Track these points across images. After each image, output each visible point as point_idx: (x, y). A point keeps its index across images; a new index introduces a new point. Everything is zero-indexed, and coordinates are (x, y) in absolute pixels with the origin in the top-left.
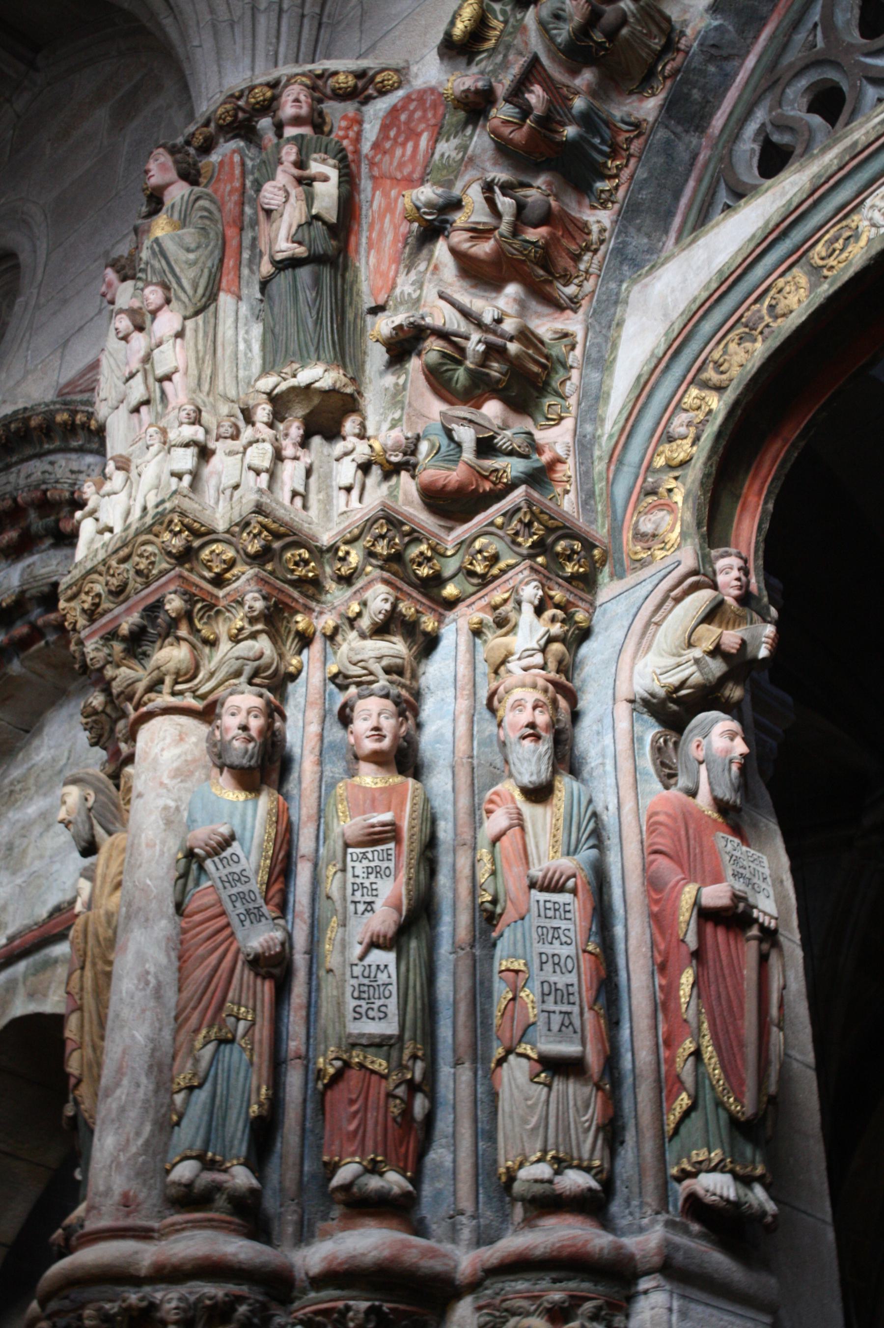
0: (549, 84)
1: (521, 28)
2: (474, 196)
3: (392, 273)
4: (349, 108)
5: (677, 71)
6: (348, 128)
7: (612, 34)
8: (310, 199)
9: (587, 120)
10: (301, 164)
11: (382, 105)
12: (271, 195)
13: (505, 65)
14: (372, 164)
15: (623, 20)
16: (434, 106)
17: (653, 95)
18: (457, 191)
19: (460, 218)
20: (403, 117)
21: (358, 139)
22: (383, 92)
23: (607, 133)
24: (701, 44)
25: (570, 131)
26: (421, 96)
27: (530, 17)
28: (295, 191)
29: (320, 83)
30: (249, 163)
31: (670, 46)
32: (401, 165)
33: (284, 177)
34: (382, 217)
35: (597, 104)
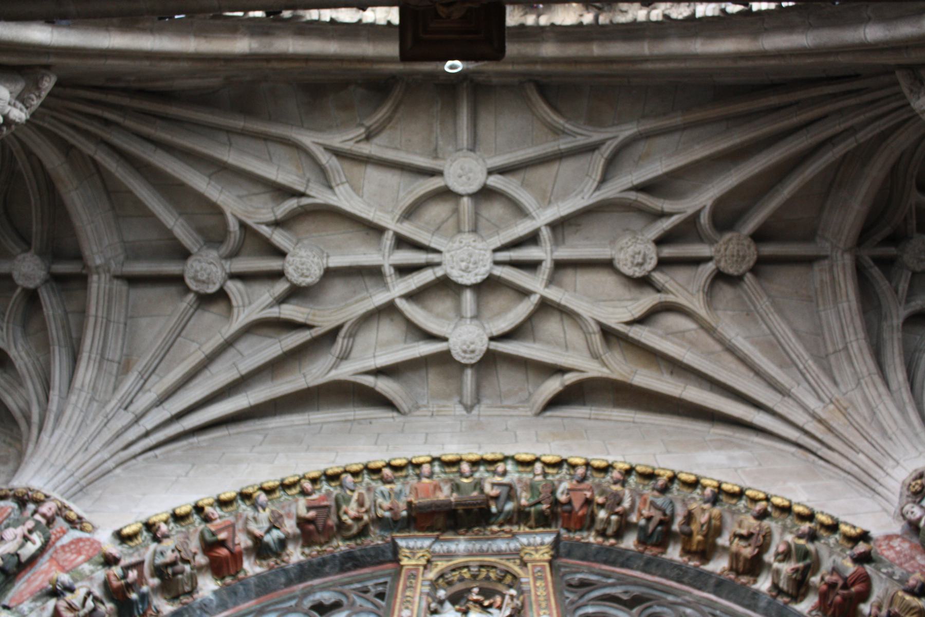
0: (141, 574)
1: (147, 547)
2: (81, 592)
3: (25, 597)
4: (66, 525)
5: (186, 604)
6: (59, 532)
7: (175, 574)
8: (22, 546)
9: (144, 597)
10: (30, 531)
11: (76, 534)
12: (9, 533)
13: (131, 555)
14: (56, 552)
15: (182, 572)
16: (95, 549)
17: (172, 605)
18: (76, 586)
19: (69, 596)
20: (81, 544)
21: (58, 539)
22: (82, 529)
23: (146, 606)
24: (201, 601)
25: (134, 596)
26: (93, 542)
27: (153, 546)
28: (20, 539)
29: (63, 509)
30: (12, 516)
31: (190, 593)
32: (65, 560)
33: (21, 530)
34: (42, 573)
35: (151, 593)
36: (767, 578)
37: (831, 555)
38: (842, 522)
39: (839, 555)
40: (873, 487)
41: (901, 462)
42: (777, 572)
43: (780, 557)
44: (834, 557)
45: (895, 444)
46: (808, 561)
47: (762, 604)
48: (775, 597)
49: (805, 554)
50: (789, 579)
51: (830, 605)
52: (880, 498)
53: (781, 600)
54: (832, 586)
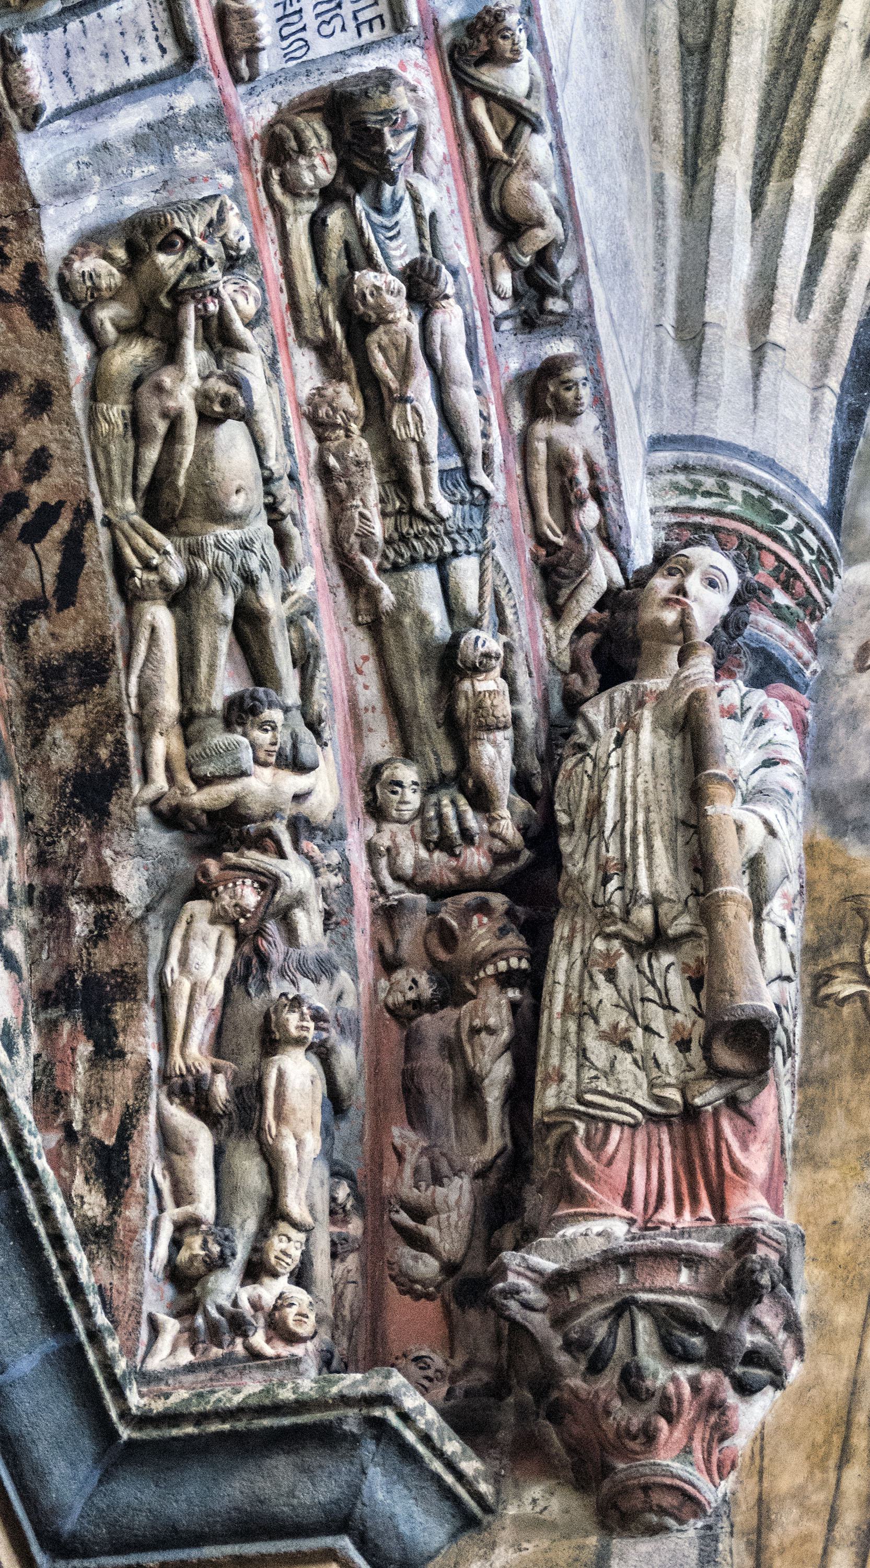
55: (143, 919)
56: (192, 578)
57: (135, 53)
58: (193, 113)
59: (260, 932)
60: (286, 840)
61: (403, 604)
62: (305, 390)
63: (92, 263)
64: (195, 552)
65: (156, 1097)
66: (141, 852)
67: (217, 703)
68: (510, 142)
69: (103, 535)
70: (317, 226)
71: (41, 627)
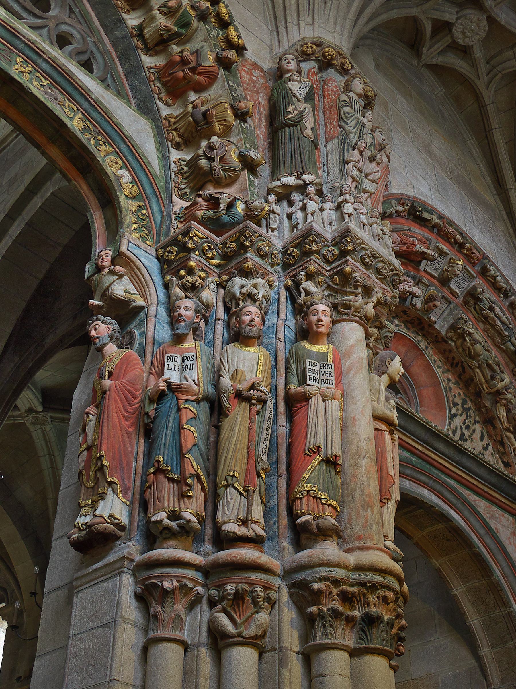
36: (139, 17)
37: (205, 40)
38: (234, 25)
39: (210, 46)
40: (279, 25)
41: (316, 24)
42: (153, 19)
43: (165, 10)
44: (204, 44)
45: (324, 10)
46: (183, 31)
47: (118, 33)
48: (132, 36)
49: (185, 24)
50: (157, 31)
51: (170, 74)
52: (276, 36)
53: (136, 42)
54: (184, 62)
55: (492, 409)
56: (479, 364)
57: (443, 307)
58: (454, 307)
59: (508, 405)
60: (506, 392)
61: (507, 348)
62: (482, 328)
63: (450, 334)
64: (478, 361)
65: (504, 432)
66: (488, 399)
67: (490, 378)
68: (495, 280)
69: (466, 363)
70: (475, 309)
71: (462, 377)
